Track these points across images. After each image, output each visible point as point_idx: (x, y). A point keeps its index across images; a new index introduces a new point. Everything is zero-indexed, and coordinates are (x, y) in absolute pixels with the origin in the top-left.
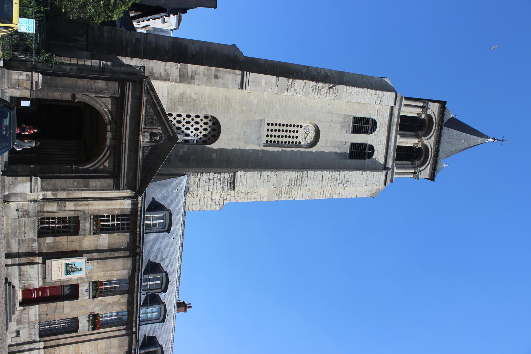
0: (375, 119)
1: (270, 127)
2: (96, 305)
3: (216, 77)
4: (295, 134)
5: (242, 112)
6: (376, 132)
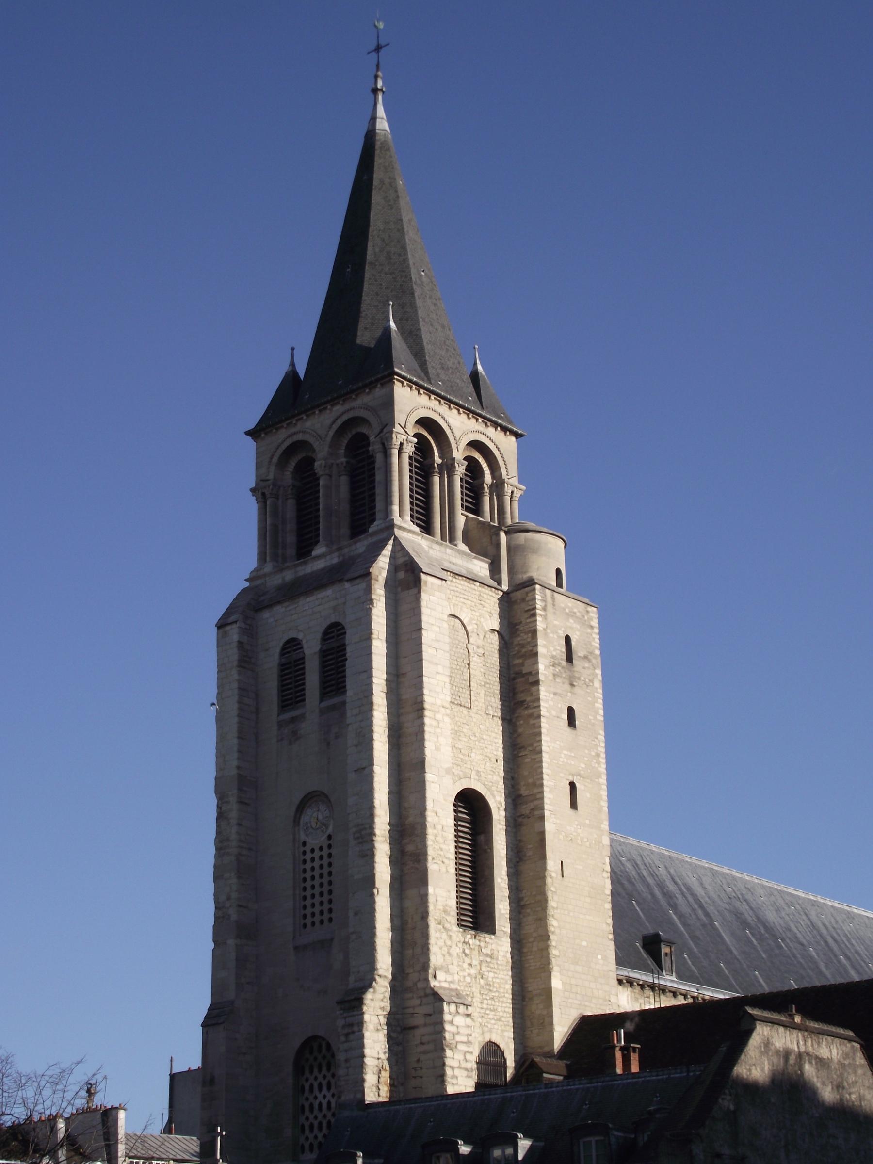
0: (278, 650)
1: (309, 921)
4: (317, 854)
6: (300, 636)
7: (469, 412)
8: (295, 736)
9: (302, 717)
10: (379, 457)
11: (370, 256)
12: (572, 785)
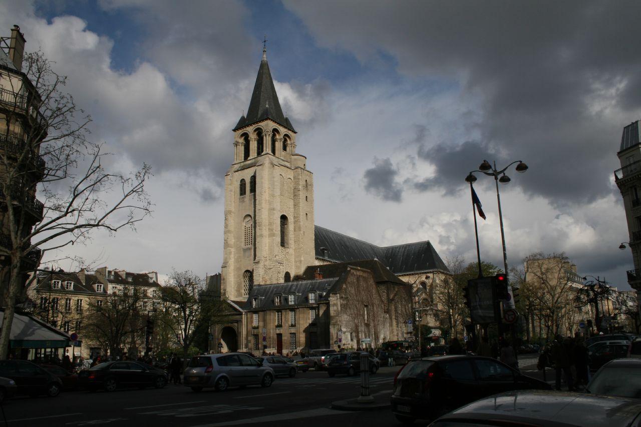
2: (285, 326)
3: (224, 279)
5: (241, 261)
7: (284, 127)
8: (243, 201)
9: (245, 197)
10: (265, 137)
11: (262, 90)
12: (306, 214)
